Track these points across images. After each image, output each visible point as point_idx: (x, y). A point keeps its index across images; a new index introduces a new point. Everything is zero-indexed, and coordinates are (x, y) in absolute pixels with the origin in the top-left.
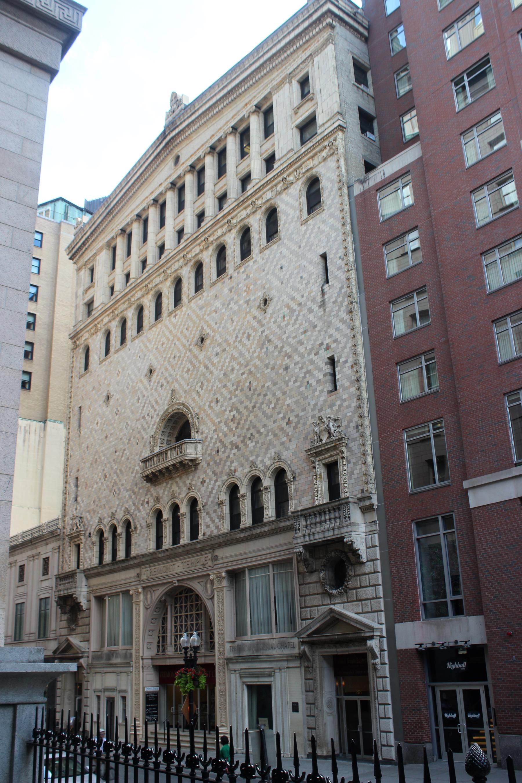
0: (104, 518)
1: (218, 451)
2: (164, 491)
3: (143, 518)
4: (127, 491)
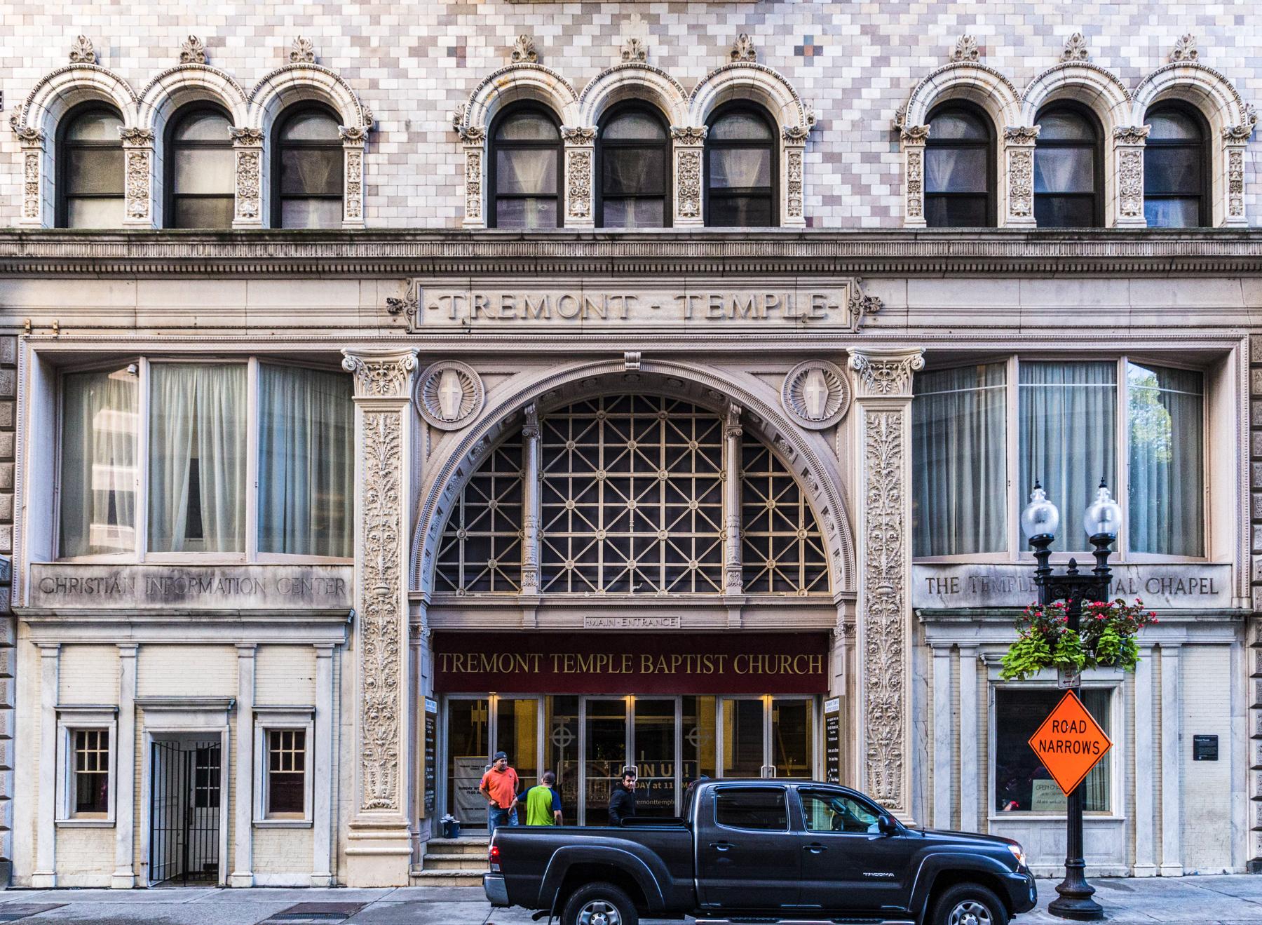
0: (115, 53)
2: (568, 34)
3: (427, 105)
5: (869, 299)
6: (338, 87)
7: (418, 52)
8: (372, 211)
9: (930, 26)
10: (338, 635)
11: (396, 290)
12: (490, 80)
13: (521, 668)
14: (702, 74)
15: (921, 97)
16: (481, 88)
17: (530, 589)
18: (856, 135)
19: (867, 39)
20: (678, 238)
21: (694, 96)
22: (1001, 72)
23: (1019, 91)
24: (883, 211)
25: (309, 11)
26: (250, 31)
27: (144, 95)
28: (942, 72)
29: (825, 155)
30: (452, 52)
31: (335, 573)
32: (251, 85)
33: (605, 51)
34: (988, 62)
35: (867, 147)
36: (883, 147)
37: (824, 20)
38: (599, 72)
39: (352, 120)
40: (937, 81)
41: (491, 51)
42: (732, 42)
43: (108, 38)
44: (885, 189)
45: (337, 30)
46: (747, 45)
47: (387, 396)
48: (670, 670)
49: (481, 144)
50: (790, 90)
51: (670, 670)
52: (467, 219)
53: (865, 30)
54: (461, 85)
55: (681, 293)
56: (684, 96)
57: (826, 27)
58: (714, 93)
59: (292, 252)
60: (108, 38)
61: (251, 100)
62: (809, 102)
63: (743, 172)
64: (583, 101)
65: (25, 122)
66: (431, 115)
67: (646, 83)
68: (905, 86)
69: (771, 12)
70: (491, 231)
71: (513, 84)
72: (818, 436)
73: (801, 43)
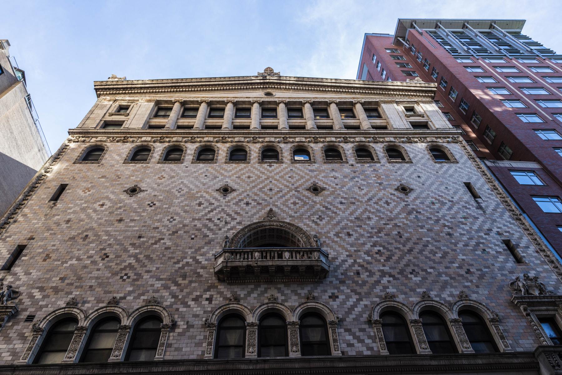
0: (84, 302)
1: (358, 273)
2: (249, 294)
3: (196, 316)
4: (159, 279)
6: (164, 312)
7: (196, 299)
8: (168, 353)
14: (297, 304)
15: (376, 310)
16: (217, 310)
18: (356, 323)
19: (353, 293)
21: (294, 311)
22: (402, 302)
25: (159, 289)
26: (136, 295)
27: (90, 315)
28: (382, 302)
29: (345, 329)
30: (207, 299)
32: (131, 311)
33: (262, 298)
34: (397, 300)
35: (360, 327)
36: (365, 326)
37: (338, 288)
38: (260, 304)
39: (167, 321)
40: (381, 305)
41: (221, 299)
43: (84, 298)
45: (167, 294)
49: (215, 328)
50: (329, 308)
52: (206, 355)
53: (352, 291)
54: (209, 309)
60: (84, 298)
61: (130, 316)
62: (336, 313)
63: (315, 336)
64: (254, 313)
65: (39, 325)
69: (319, 286)
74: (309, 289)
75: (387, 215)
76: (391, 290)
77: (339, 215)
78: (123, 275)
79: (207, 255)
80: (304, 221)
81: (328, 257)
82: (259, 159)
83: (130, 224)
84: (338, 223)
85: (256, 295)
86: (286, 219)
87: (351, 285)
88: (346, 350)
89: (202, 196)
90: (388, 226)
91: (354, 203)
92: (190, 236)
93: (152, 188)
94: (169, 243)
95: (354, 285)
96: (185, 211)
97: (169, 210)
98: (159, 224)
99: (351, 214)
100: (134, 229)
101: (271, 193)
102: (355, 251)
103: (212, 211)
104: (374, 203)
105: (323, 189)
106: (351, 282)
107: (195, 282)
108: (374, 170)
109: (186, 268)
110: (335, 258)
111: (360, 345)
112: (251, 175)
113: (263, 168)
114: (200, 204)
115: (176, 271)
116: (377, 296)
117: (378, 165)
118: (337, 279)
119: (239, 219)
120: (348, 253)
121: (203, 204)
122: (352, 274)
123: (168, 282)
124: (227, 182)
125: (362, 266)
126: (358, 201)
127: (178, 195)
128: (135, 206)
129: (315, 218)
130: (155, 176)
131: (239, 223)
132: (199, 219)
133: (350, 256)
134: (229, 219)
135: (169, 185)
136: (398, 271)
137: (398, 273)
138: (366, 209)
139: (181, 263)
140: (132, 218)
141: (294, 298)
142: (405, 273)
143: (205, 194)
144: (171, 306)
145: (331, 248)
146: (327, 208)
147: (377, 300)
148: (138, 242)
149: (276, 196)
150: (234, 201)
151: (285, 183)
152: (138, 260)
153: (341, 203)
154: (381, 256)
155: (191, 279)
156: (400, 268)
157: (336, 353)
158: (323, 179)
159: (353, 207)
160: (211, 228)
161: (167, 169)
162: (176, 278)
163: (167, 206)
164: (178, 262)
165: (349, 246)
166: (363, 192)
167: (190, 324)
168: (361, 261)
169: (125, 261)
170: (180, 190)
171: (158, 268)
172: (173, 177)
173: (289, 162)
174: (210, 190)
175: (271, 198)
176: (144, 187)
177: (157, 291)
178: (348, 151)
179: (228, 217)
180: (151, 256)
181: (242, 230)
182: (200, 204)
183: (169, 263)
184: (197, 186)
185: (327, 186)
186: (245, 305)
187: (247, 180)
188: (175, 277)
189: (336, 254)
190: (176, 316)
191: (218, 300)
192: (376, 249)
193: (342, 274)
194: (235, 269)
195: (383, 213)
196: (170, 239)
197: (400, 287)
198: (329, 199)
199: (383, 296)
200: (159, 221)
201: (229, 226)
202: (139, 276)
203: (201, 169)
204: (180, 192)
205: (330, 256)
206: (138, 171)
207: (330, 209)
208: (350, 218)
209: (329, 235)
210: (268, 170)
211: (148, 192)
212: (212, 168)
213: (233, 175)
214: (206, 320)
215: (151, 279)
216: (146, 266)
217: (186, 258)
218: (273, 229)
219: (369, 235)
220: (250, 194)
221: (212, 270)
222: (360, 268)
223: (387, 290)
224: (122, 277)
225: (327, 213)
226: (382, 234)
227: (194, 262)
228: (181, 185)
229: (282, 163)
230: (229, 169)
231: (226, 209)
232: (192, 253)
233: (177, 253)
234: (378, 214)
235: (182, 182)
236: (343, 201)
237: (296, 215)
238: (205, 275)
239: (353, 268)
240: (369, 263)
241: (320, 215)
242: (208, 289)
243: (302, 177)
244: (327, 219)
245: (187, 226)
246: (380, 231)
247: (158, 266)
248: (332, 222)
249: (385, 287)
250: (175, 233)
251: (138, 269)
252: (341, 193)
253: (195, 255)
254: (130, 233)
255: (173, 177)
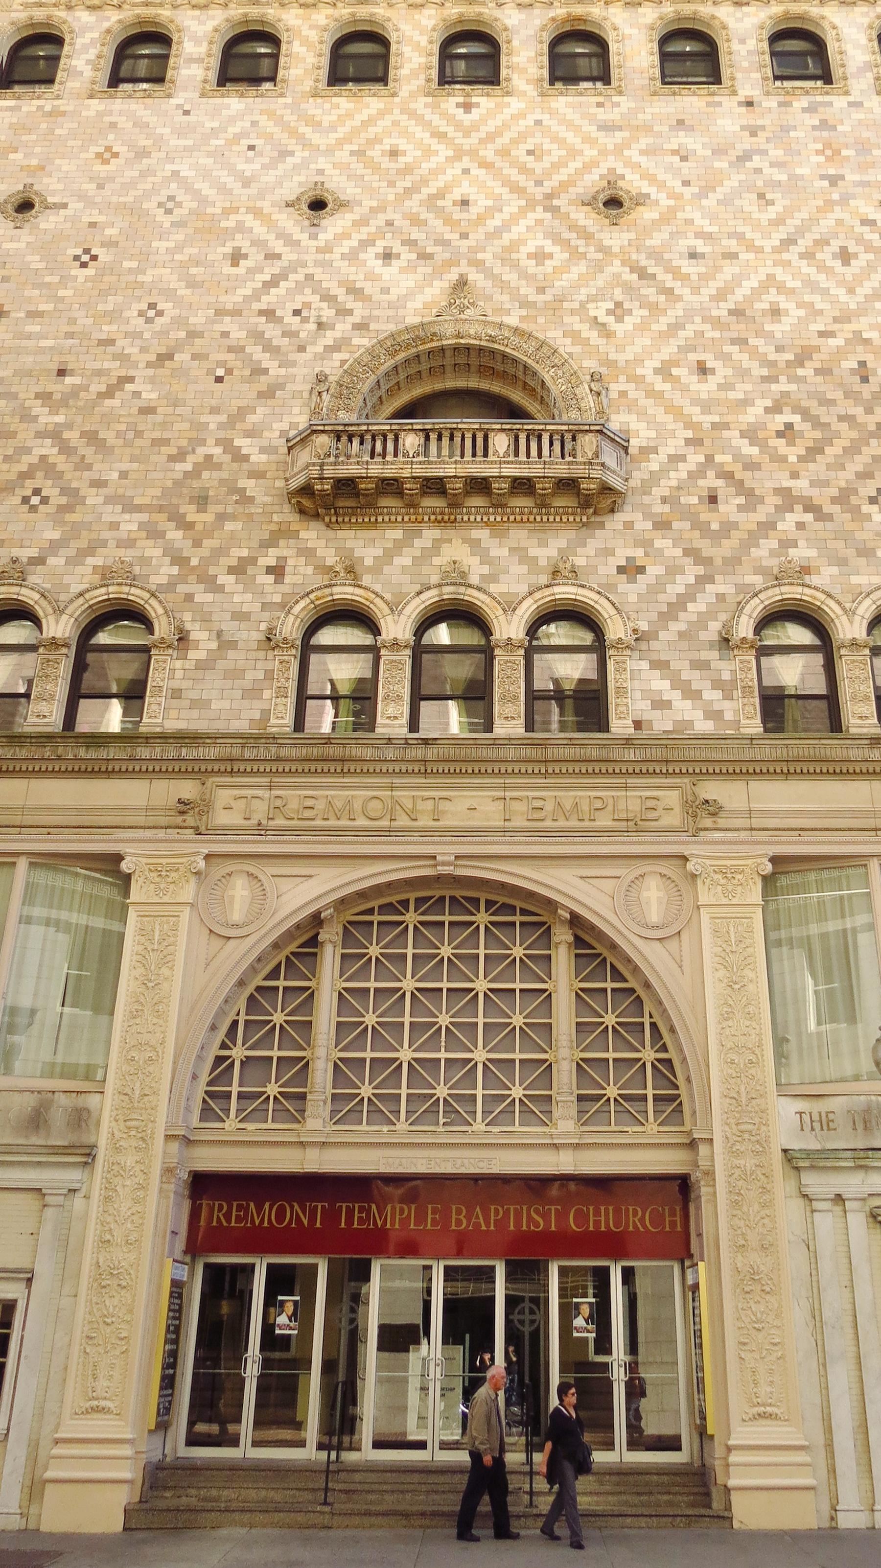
1: (713, 499)
2: (389, 556)
3: (240, 616)
4: (130, 507)
5: (707, 801)
6: (153, 601)
8: (173, 713)
9: (752, 550)
10: (73, 1176)
11: (187, 789)
12: (308, 594)
13: (299, 1220)
14: (523, 589)
15: (748, 609)
16: (297, 602)
17: (317, 1119)
18: (684, 645)
19: (690, 560)
20: (496, 743)
21: (514, 610)
23: (848, 606)
24: (715, 715)
25: (133, 536)
26: (72, 552)
28: (767, 589)
30: (270, 570)
31: (81, 1101)
32: (63, 597)
33: (425, 570)
34: (815, 580)
35: (695, 655)
37: (646, 544)
38: (418, 588)
39: (162, 628)
40: (762, 596)
41: (310, 570)
42: (553, 562)
44: (717, 695)
45: (158, 552)
46: (568, 565)
47: (166, 899)
48: (488, 1224)
49: (294, 652)
50: (613, 604)
51: (488, 1224)
52: (273, 721)
53: (687, 552)
54: (277, 598)
55: (501, 794)
56: (504, 610)
57: (649, 549)
58: (535, 606)
59: (82, 753)
61: (62, 612)
62: (633, 615)
66: (243, 625)
67: (466, 598)
68: (732, 600)
70: (297, 735)
71: (330, 598)
72: (657, 944)
73: (623, 563)
74: (562, 543)
75: (835, 302)
76: (802, 553)
77: (680, 298)
78: (29, 492)
79: (266, 434)
80: (566, 320)
81: (626, 449)
82: (429, 80)
83: (30, 328)
84: (675, 327)
85: (407, 561)
86: (508, 312)
87: (686, 536)
88: (646, 717)
89: (240, 227)
90: (831, 342)
91: (734, 256)
92: (211, 371)
93: (82, 196)
94: (149, 395)
95: (697, 533)
96: (192, 284)
97: (140, 278)
98: (114, 328)
99: (720, 296)
100: (44, 343)
101: (465, 215)
102: (714, 425)
103: (274, 282)
104: (802, 256)
105: (641, 200)
106: (687, 525)
107: (233, 517)
108: (824, 125)
109: (205, 475)
110: (647, 451)
111: (688, 703)
112: (402, 144)
113: (444, 115)
114: (236, 258)
115: (176, 482)
116: (759, 570)
117: (839, 102)
118: (647, 516)
119: (359, 312)
120: (690, 434)
121: (245, 256)
122: (695, 500)
123: (156, 517)
124: (321, 172)
125: (728, 476)
126: (751, 247)
127: (167, 225)
128: (35, 261)
129: (600, 310)
130: (84, 148)
131: (361, 327)
132: (236, 313)
133: (694, 442)
134: (328, 313)
135: (133, 184)
136: (834, 492)
137: (834, 500)
138: (771, 277)
139: (191, 458)
140: (32, 308)
141: (518, 569)
142: (854, 500)
143: (249, 220)
144: (171, 586)
145: (642, 414)
146: (643, 274)
147: (757, 580)
148: (59, 387)
149: (481, 229)
150: (345, 246)
151: (513, 174)
152: (65, 449)
153: (693, 256)
154: (791, 443)
155: (220, 508)
156: (843, 484)
157: (620, 725)
158: (643, 160)
159: (729, 270)
160: (275, 343)
161: (124, 123)
162: (178, 506)
163: (134, 264)
164: (180, 456)
165: (698, 409)
166: (772, 212)
167: (226, 637)
168: (728, 458)
169: (28, 451)
170: (170, 205)
171: (124, 475)
172: (143, 153)
173: (531, 90)
174: (266, 205)
175: (464, 236)
176: (54, 193)
177: (129, 543)
178: (743, 41)
179: (325, 305)
180: (101, 435)
181: (370, 351)
182: (236, 258)
183: (154, 458)
184: (223, 189)
185: (652, 191)
186: (378, 588)
187: (386, 163)
188: (175, 501)
189: (653, 434)
190: (187, 617)
191: (301, 573)
192: (780, 420)
193: (664, 500)
194: (346, 486)
195: (825, 292)
196: (152, 380)
197: (831, 544)
198: (656, 240)
199: (776, 571)
200: (112, 316)
201: (329, 338)
202: (74, 499)
203: (232, 120)
204: (169, 212)
205: (633, 442)
206: (30, 131)
207: (654, 276)
208: (715, 313)
209: (639, 371)
210: (458, 126)
211: (68, 212)
212: (271, 114)
213: (340, 143)
214: (271, 630)
215: (110, 507)
216: (89, 467)
217: (203, 442)
218: (468, 348)
219: (765, 372)
220: (397, 219)
221: (280, 484)
222: (720, 483)
223: (792, 551)
224: (26, 500)
225: (643, 291)
226: (806, 372)
227: (227, 458)
228: (174, 186)
229: (508, 94)
230: (326, 120)
231: (319, 274)
232: (221, 426)
233: (176, 427)
234: (807, 298)
235: (175, 173)
236: (701, 246)
237: (541, 298)
238: (262, 498)
239: (701, 482)
240: (751, 466)
241: (620, 298)
242: (271, 542)
243: (573, 153)
244: (639, 313)
245: (200, 334)
246: (800, 362)
247: (125, 466)
248: (654, 327)
249: (787, 544)
250: (165, 357)
251: (68, 476)
252: (697, 216)
253: (229, 434)
254: (31, 359)
255: (143, 153)
